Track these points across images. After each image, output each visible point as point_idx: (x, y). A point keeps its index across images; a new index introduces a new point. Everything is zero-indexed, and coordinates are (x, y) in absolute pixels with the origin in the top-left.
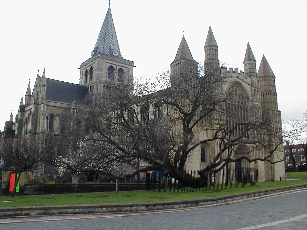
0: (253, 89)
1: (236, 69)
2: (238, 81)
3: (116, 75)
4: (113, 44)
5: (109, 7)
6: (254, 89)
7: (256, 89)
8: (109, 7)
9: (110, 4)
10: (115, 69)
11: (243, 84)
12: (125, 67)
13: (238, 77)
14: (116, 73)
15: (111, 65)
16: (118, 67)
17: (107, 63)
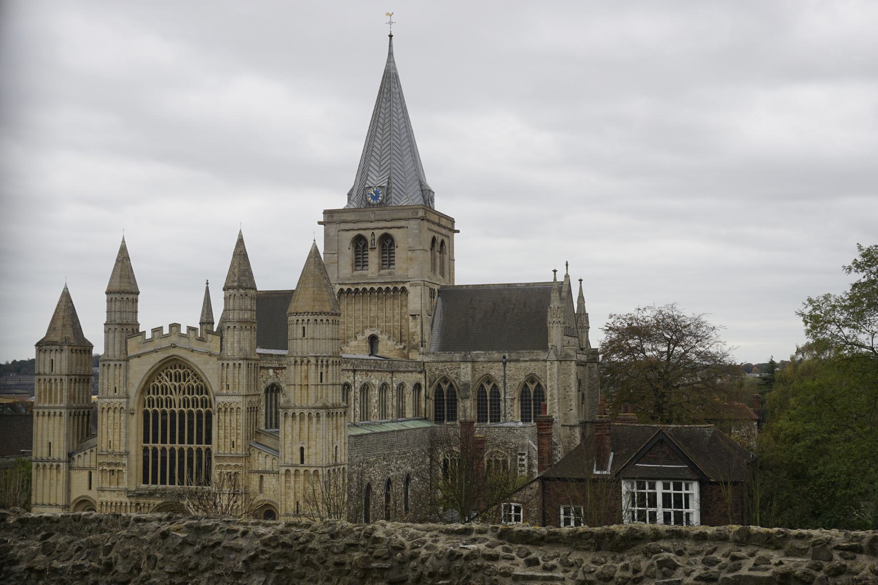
0: (221, 364)
1: (175, 326)
2: (174, 355)
3: (373, 257)
4: (377, 169)
5: (391, 54)
6: (223, 364)
7: (228, 364)
8: (391, 54)
9: (390, 46)
10: (369, 238)
11: (194, 359)
12: (399, 228)
13: (174, 346)
14: (373, 251)
15: (356, 233)
16: (378, 233)
17: (347, 230)
